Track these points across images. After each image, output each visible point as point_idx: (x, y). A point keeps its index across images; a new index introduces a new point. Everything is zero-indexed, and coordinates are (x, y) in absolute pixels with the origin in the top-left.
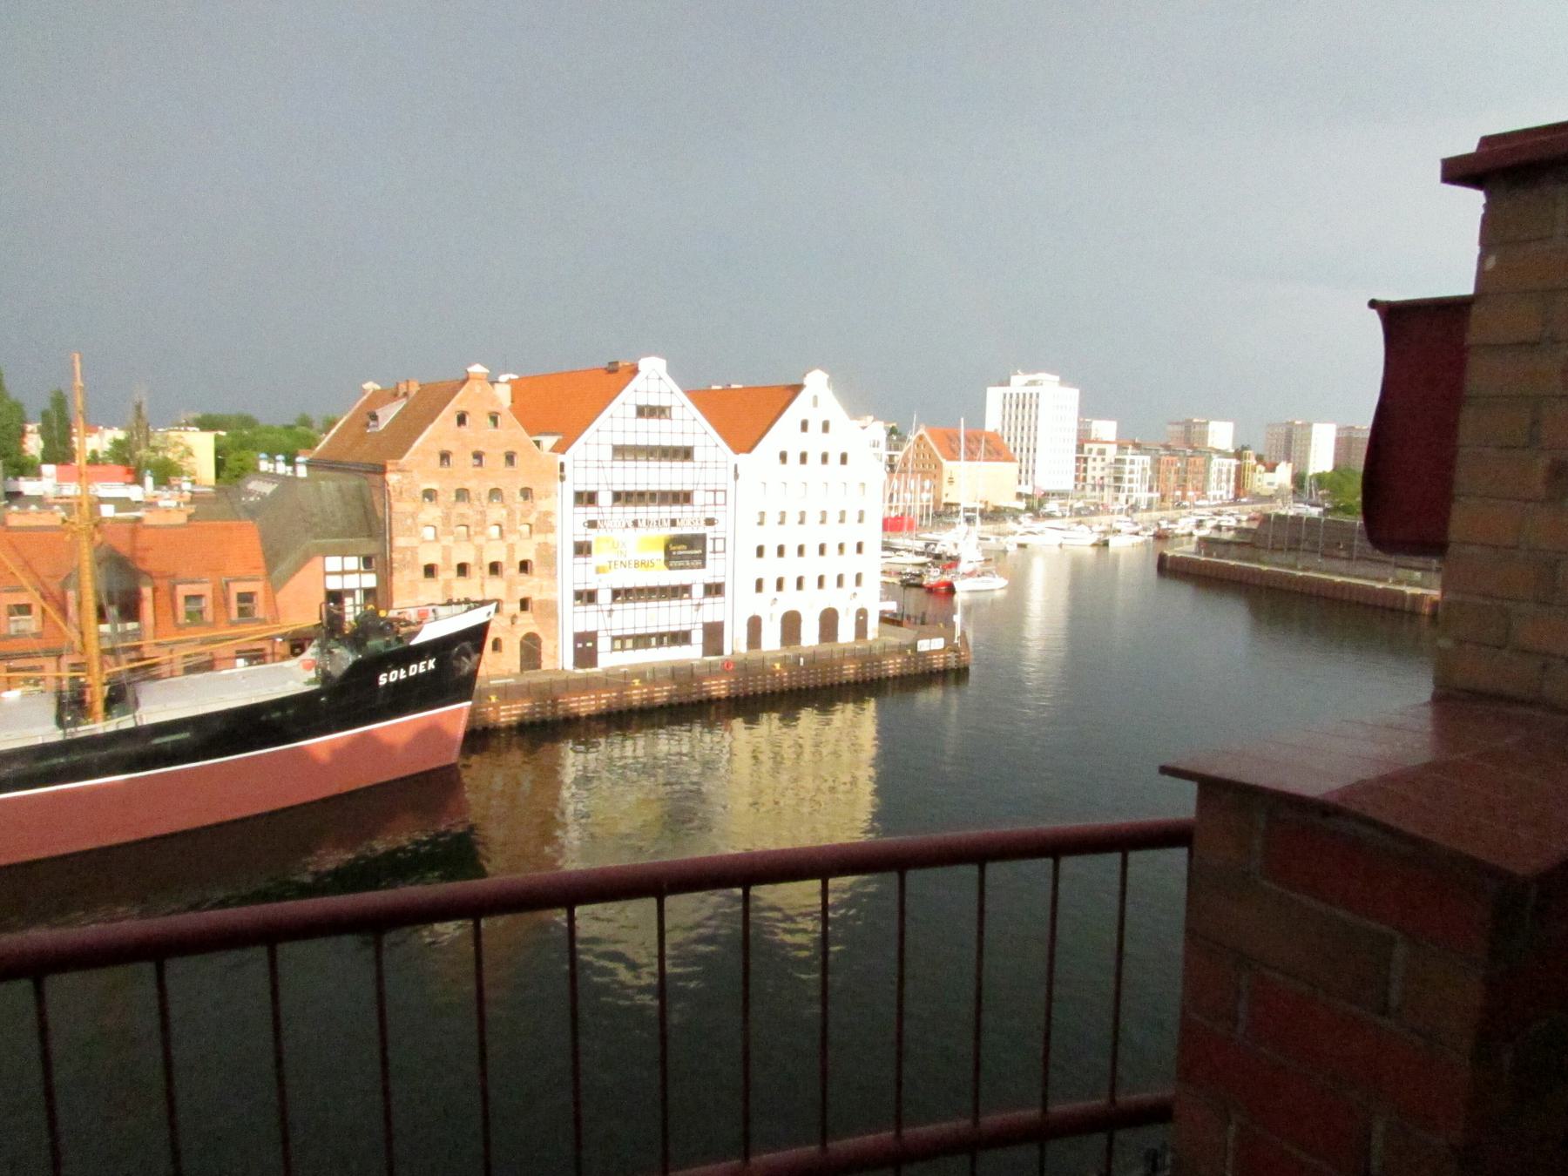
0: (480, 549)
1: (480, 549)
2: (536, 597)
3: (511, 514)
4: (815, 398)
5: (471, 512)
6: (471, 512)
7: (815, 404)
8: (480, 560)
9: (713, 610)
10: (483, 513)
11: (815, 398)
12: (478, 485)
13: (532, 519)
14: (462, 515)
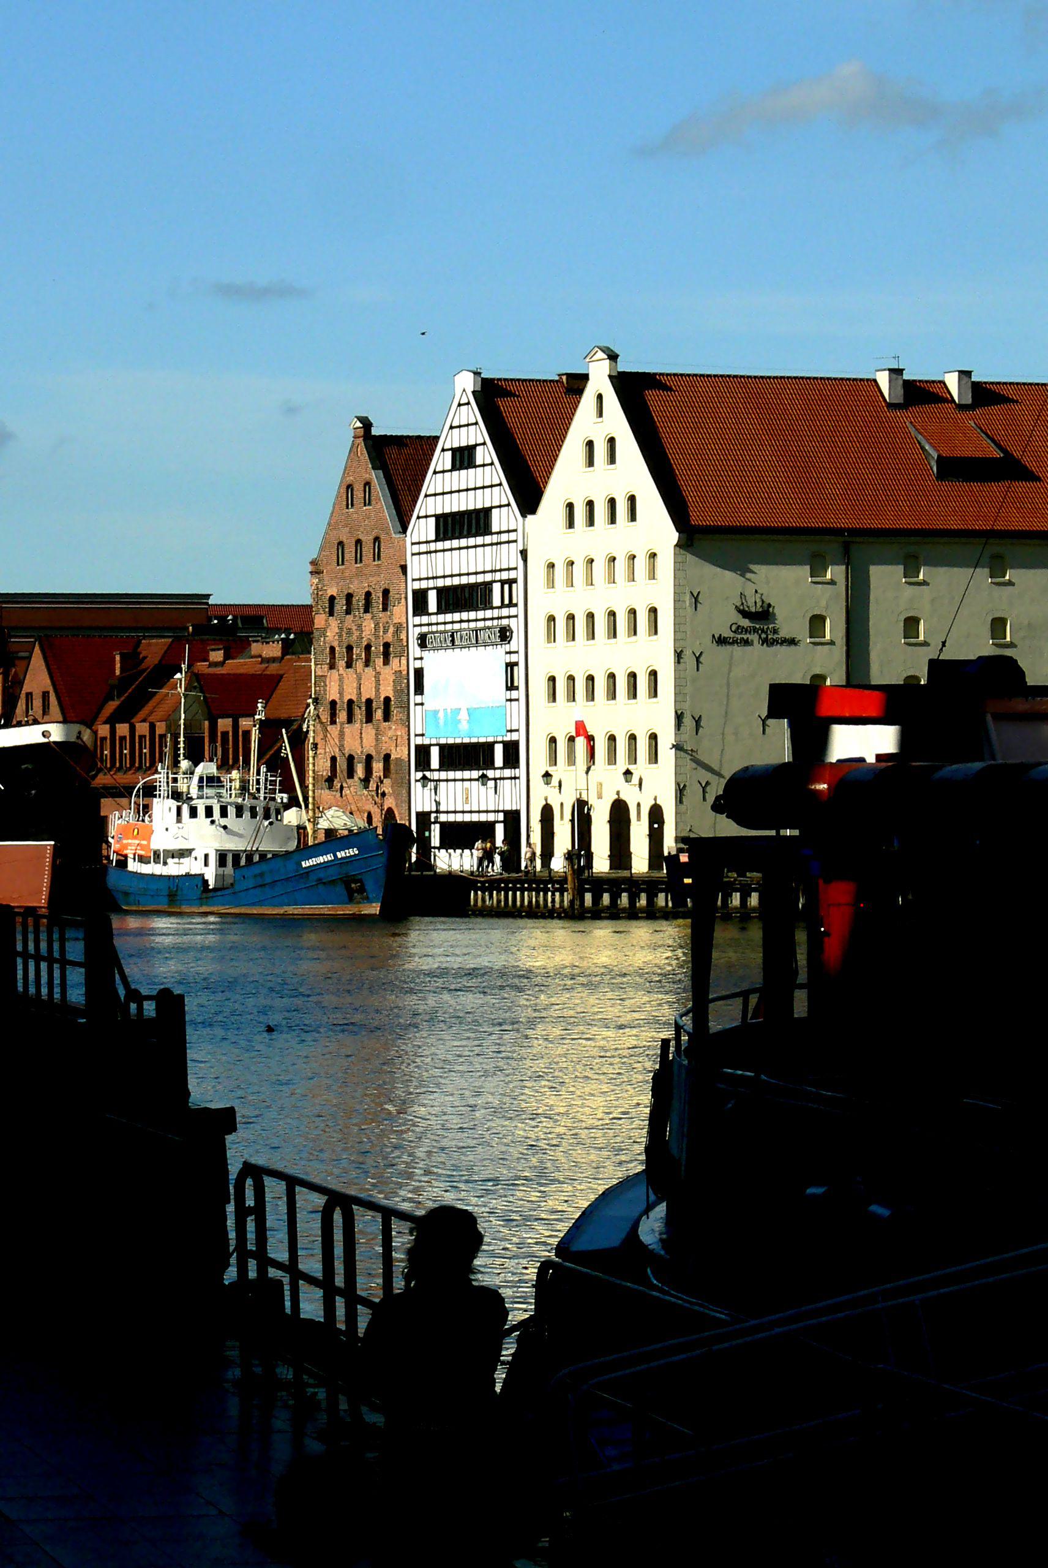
0: (359, 679)
1: (359, 679)
2: (393, 757)
3: (377, 625)
4: (600, 397)
5: (354, 628)
6: (354, 628)
7: (600, 414)
8: (360, 694)
9: (510, 797)
10: (360, 627)
11: (600, 397)
12: (358, 589)
13: (389, 637)
14: (349, 630)
